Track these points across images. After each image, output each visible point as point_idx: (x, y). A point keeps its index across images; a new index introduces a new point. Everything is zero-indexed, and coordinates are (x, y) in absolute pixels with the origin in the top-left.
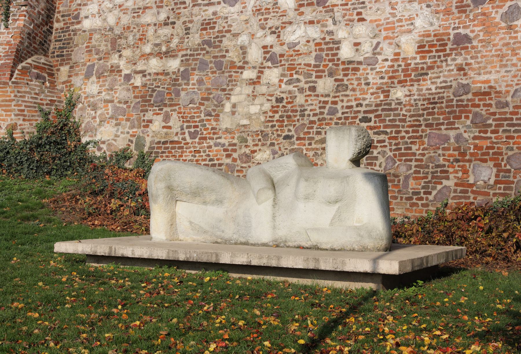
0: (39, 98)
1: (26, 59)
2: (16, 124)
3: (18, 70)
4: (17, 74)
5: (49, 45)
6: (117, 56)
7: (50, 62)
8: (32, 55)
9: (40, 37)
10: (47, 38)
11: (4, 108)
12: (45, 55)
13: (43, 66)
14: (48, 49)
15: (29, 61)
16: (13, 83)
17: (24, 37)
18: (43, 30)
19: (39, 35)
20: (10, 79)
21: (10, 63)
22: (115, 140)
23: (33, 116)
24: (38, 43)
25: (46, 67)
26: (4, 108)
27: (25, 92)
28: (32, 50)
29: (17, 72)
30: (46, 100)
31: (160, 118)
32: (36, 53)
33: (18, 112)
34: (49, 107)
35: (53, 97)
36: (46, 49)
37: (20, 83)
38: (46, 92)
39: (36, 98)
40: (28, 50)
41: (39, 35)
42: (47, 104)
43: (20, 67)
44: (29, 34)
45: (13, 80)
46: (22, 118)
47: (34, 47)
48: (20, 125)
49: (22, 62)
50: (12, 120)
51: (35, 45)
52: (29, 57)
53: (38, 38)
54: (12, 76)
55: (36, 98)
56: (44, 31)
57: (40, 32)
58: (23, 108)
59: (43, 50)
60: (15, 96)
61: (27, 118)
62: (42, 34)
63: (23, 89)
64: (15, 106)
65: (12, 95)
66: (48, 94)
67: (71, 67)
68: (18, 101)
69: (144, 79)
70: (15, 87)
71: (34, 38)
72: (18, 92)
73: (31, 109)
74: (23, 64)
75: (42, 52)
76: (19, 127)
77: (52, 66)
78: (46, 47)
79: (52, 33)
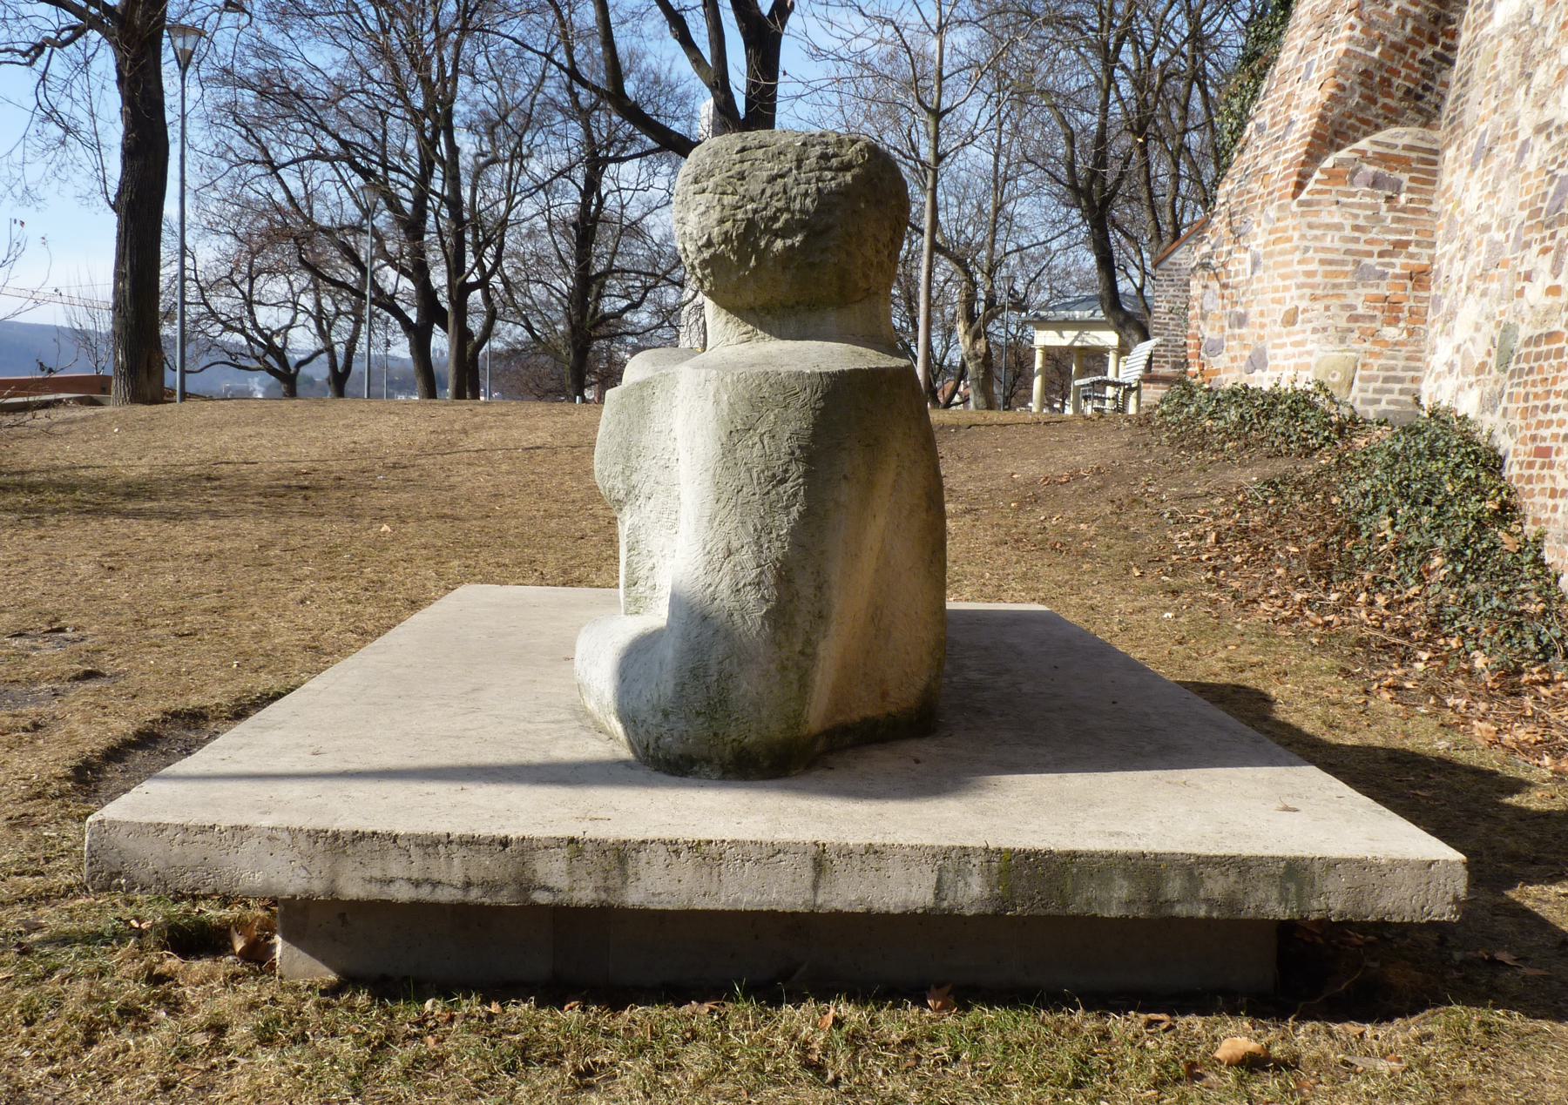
0: (1364, 237)
1: (1356, 140)
2: (1297, 308)
3: (1323, 171)
4: (1317, 181)
5: (1443, 97)
6: (1522, 91)
7: (1436, 141)
8: (1378, 128)
9: (1407, 77)
10: (1433, 78)
11: (1282, 271)
12: (1425, 125)
13: (1403, 153)
14: (1438, 107)
15: (1363, 144)
16: (1301, 204)
17: (1347, 84)
18: (1420, 56)
19: (1404, 72)
20: (1295, 196)
21: (1300, 155)
22: (1473, 340)
23: (1335, 286)
24: (1400, 94)
25: (1414, 155)
26: (1282, 271)
27: (1328, 226)
28: (1377, 116)
29: (1317, 175)
30: (1381, 242)
31: (1546, 263)
32: (1396, 123)
33: (1302, 279)
34: (1386, 260)
35: (1407, 232)
36: (1431, 108)
37: (1319, 203)
38: (1389, 220)
39: (1357, 240)
40: (1360, 115)
41: (1404, 72)
42: (1381, 254)
43: (1328, 163)
44: (1366, 74)
45: (1304, 196)
46: (1308, 291)
47: (1385, 106)
48: (1305, 311)
49: (1339, 147)
50: (1292, 298)
51: (1387, 101)
52: (1366, 134)
53: (1397, 81)
54: (1300, 186)
55: (1357, 240)
56: (1422, 61)
57: (1406, 65)
58: (1314, 266)
59: (1420, 111)
60: (1303, 237)
61: (1319, 292)
62: (1416, 70)
63: (1325, 218)
64: (1299, 262)
65: (1296, 235)
66: (1394, 226)
67: (1458, 149)
68: (1306, 250)
69: (1548, 146)
70: (1303, 214)
71: (1386, 82)
72: (1310, 226)
73: (1334, 268)
74: (1343, 154)
75: (1416, 116)
76: (1300, 317)
77: (1436, 152)
78: (1429, 102)
79: (1451, 63)
